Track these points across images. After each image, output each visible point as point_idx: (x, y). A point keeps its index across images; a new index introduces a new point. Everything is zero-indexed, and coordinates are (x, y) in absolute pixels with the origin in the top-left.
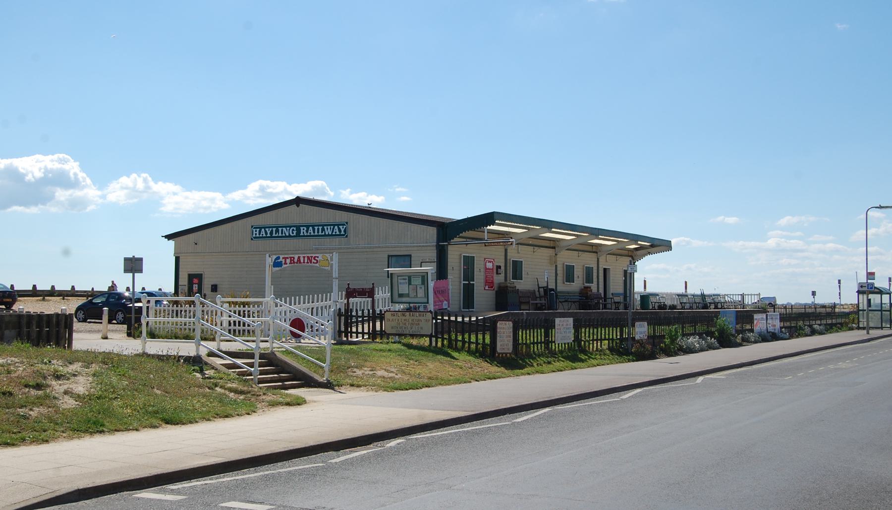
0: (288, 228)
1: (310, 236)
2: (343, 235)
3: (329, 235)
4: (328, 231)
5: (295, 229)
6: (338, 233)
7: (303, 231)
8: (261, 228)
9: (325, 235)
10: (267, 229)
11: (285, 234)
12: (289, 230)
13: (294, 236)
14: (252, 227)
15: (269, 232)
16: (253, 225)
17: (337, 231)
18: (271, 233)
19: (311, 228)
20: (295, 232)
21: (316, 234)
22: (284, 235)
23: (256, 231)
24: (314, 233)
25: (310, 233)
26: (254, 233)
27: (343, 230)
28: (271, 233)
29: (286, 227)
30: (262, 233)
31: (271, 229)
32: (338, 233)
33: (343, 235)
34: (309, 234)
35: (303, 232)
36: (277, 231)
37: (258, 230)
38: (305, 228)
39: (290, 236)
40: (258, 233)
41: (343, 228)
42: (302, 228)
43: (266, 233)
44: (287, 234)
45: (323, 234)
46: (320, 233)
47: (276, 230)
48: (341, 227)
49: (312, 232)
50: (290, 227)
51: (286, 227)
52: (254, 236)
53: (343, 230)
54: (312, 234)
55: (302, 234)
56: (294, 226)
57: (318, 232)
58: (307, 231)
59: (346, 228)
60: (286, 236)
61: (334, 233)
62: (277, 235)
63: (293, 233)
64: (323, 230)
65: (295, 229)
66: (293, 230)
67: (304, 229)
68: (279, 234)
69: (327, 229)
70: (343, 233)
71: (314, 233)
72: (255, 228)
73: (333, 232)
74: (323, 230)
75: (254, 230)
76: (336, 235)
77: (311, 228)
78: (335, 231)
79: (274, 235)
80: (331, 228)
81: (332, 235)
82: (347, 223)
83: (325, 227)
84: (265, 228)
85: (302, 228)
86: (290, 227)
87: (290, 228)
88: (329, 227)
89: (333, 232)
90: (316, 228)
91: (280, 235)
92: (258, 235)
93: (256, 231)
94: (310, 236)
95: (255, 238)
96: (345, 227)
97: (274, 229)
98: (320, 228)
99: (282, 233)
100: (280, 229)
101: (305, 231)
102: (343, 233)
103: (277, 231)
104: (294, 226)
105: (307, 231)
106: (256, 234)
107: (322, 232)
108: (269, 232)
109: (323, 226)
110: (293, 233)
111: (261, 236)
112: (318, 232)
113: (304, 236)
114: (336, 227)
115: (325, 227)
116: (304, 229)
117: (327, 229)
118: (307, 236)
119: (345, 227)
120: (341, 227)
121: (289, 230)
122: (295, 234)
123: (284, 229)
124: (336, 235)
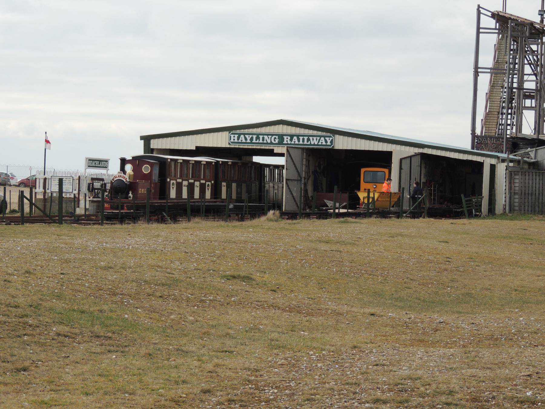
5: (277, 137)
10: (247, 136)
11: (266, 141)
12: (271, 138)
13: (276, 144)
18: (252, 139)
19: (295, 138)
20: (277, 141)
22: (265, 142)
23: (234, 137)
24: (299, 141)
26: (232, 138)
28: (252, 139)
29: (268, 135)
30: (240, 139)
35: (287, 141)
36: (258, 138)
37: (236, 136)
38: (289, 138)
40: (236, 138)
41: (249, 137)
43: (246, 139)
44: (269, 142)
45: (309, 143)
49: (296, 141)
50: (272, 135)
51: (268, 135)
52: (232, 140)
55: (285, 142)
56: (276, 135)
58: (291, 140)
59: (332, 140)
62: (258, 141)
64: (308, 140)
65: (277, 137)
66: (275, 138)
67: (287, 138)
68: (259, 141)
69: (313, 139)
71: (299, 141)
73: (319, 142)
74: (308, 140)
75: (232, 136)
77: (295, 138)
78: (321, 141)
79: (254, 141)
80: (317, 139)
83: (311, 138)
85: (285, 137)
86: (272, 135)
88: (315, 138)
89: (319, 142)
90: (301, 138)
91: (261, 141)
92: (236, 141)
93: (234, 137)
96: (331, 139)
97: (255, 137)
98: (306, 138)
100: (261, 137)
101: (288, 140)
103: (258, 138)
104: (276, 135)
106: (234, 140)
107: (308, 142)
110: (275, 141)
111: (240, 141)
113: (288, 144)
115: (311, 138)
117: (313, 139)
118: (291, 144)
119: (331, 139)
121: (271, 138)
123: (266, 137)
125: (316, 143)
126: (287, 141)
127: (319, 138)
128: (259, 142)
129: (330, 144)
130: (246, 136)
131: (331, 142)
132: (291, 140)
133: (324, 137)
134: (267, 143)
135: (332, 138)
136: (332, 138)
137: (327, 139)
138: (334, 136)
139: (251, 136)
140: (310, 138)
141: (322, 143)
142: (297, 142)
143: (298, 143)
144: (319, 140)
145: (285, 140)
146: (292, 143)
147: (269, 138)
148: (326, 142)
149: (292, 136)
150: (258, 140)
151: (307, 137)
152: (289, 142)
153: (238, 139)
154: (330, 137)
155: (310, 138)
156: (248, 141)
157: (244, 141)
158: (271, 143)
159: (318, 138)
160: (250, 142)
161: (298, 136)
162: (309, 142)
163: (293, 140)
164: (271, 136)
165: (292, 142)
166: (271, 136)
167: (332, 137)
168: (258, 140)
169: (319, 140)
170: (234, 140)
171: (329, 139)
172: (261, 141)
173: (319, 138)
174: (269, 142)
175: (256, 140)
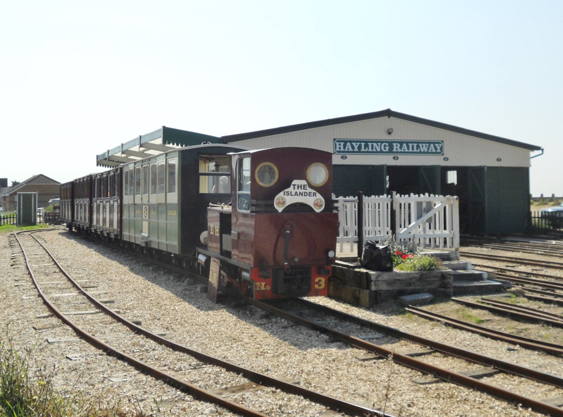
0: (379, 144)
1: (404, 152)
2: (439, 153)
3: (424, 153)
4: (424, 148)
5: (387, 144)
6: (434, 151)
7: (396, 147)
8: (345, 142)
9: (420, 152)
10: (354, 144)
11: (376, 149)
12: (381, 145)
14: (334, 140)
15: (356, 147)
16: (335, 138)
17: (433, 149)
18: (360, 147)
19: (405, 145)
20: (387, 148)
21: (411, 150)
22: (374, 150)
23: (340, 145)
24: (408, 149)
25: (404, 150)
26: (338, 147)
27: (439, 148)
28: (360, 147)
29: (377, 142)
30: (347, 147)
31: (358, 144)
32: (434, 151)
33: (439, 153)
34: (403, 151)
35: (397, 149)
36: (366, 146)
37: (342, 144)
38: (399, 145)
39: (381, 152)
40: (342, 146)
45: (419, 151)
46: (415, 150)
47: (364, 145)
48: (437, 145)
49: (406, 148)
50: (382, 142)
51: (377, 142)
52: (338, 149)
53: (439, 148)
54: (406, 150)
55: (395, 150)
56: (386, 142)
57: (413, 149)
58: (401, 147)
59: (442, 147)
60: (377, 152)
61: (430, 151)
62: (367, 150)
63: (385, 149)
64: (418, 147)
65: (387, 144)
66: (385, 146)
67: (397, 146)
68: (368, 149)
69: (423, 146)
70: (439, 151)
71: (408, 149)
72: (338, 141)
73: (428, 149)
74: (418, 147)
75: (338, 144)
76: (432, 153)
77: (405, 145)
78: (430, 148)
79: (363, 150)
80: (426, 146)
81: (427, 153)
82: (443, 142)
83: (420, 145)
84: (351, 142)
85: (394, 144)
86: (382, 142)
88: (424, 145)
89: (428, 149)
90: (410, 145)
91: (370, 150)
92: (342, 149)
93: (340, 145)
94: (404, 152)
95: (338, 152)
96: (441, 145)
97: (363, 144)
98: (415, 145)
99: (372, 148)
100: (370, 144)
101: (398, 147)
102: (439, 151)
103: (366, 146)
104: (386, 142)
105: (401, 147)
106: (340, 148)
107: (417, 149)
108: (356, 147)
109: (418, 143)
110: (385, 149)
111: (346, 150)
112: (413, 149)
114: (432, 145)
115: (420, 145)
116: (397, 146)
117: (423, 146)
118: (401, 152)
119: (441, 145)
120: (437, 145)
121: (381, 145)
122: (387, 150)
123: (375, 144)
124: (432, 153)
125: (426, 151)
126: (397, 149)
130: (353, 143)
131: (441, 149)
139: (358, 144)
141: (432, 150)
143: (408, 151)
144: (429, 147)
145: (395, 147)
147: (378, 145)
148: (436, 149)
152: (399, 150)
153: (345, 147)
156: (356, 150)
159: (428, 145)
160: (358, 150)
162: (419, 149)
170: (340, 148)
171: (439, 146)
174: (379, 150)
175: (365, 149)
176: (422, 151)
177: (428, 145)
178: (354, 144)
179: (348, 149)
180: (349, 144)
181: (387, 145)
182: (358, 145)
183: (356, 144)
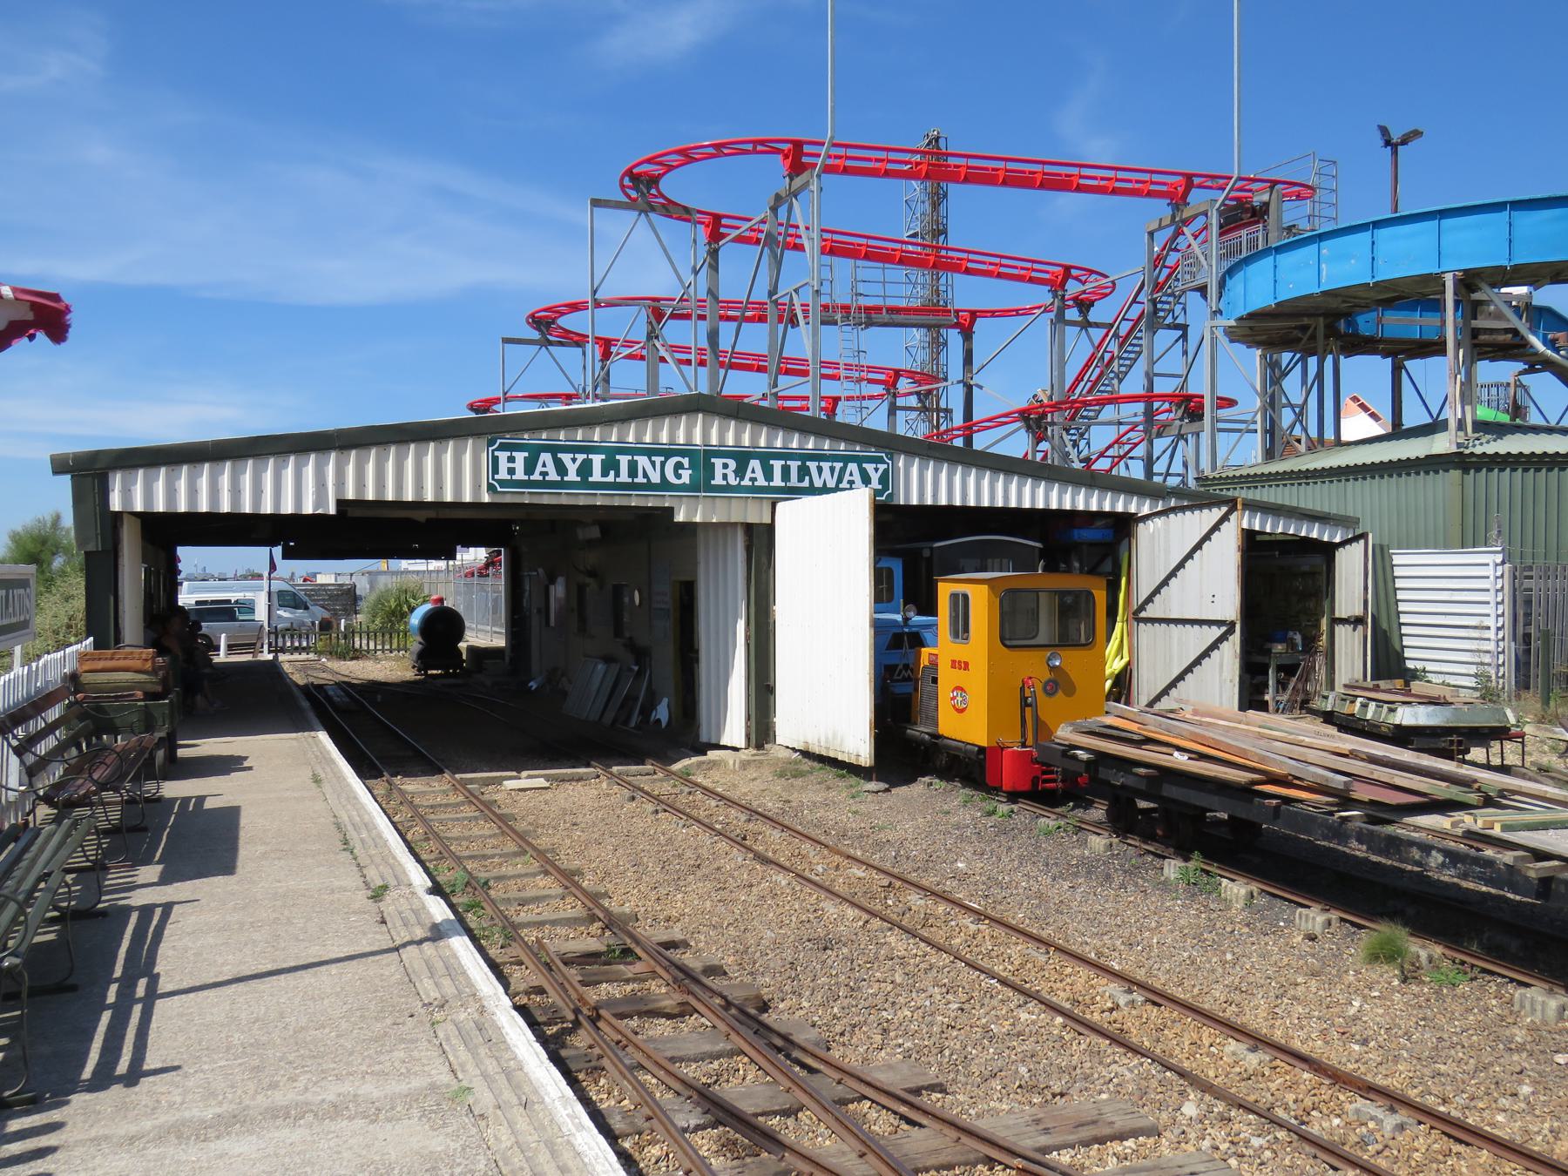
0: (658, 460)
5: (686, 462)
10: (566, 458)
11: (645, 475)
12: (663, 464)
13: (683, 488)
18: (585, 469)
19: (755, 464)
22: (640, 479)
24: (769, 475)
26: (504, 465)
28: (585, 469)
30: (539, 468)
34: (746, 482)
35: (725, 477)
37: (520, 457)
38: (732, 464)
40: (519, 465)
41: (574, 460)
42: (718, 462)
43: (561, 469)
45: (806, 484)
49: (759, 474)
50: (667, 453)
51: (649, 453)
52: (503, 474)
55: (718, 481)
56: (682, 453)
58: (740, 472)
59: (886, 471)
62: (611, 478)
63: (679, 476)
65: (686, 462)
66: (679, 466)
67: (725, 466)
68: (617, 475)
69: (820, 469)
71: (769, 475)
74: (804, 472)
75: (503, 456)
77: (755, 464)
79: (596, 476)
80: (832, 469)
83: (812, 465)
85: (718, 462)
86: (667, 453)
87: (666, 460)
88: (826, 465)
90: (777, 465)
91: (624, 477)
92: (520, 475)
93: (511, 459)
96: (882, 467)
97: (597, 460)
98: (794, 465)
100: (624, 460)
103: (610, 465)
104: (682, 453)
106: (511, 471)
107: (801, 480)
110: (679, 476)
111: (536, 477)
113: (727, 488)
115: (812, 465)
117: (820, 469)
118: (738, 489)
119: (882, 467)
121: (663, 464)
123: (642, 461)
126: (725, 477)
127: (841, 464)
128: (618, 480)
129: (880, 487)
130: (559, 455)
132: (740, 472)
133: (859, 461)
134: (649, 486)
135: (886, 466)
136: (886, 466)
137: (869, 467)
138: (891, 459)
139: (581, 457)
140: (808, 463)
142: (761, 482)
143: (766, 484)
144: (843, 470)
145: (719, 471)
146: (743, 483)
147: (653, 463)
149: (742, 458)
150: (612, 473)
151: (800, 463)
152: (733, 481)
153: (530, 467)
154: (880, 460)
155: (808, 463)
156: (572, 476)
157: (553, 476)
158: (665, 485)
159: (838, 465)
161: (765, 458)
162: (807, 478)
163: (749, 474)
164: (663, 459)
165: (742, 478)
166: (663, 459)
167: (885, 463)
168: (612, 473)
169: (843, 470)
170: (511, 471)
171: (876, 470)
172: (624, 477)
173: (841, 464)
174: (655, 478)
175: (605, 473)
176: (818, 483)
177: (838, 465)
178: (566, 458)
179: (544, 474)
180: (546, 457)
181: (686, 466)
182: (578, 463)
183: (574, 460)
